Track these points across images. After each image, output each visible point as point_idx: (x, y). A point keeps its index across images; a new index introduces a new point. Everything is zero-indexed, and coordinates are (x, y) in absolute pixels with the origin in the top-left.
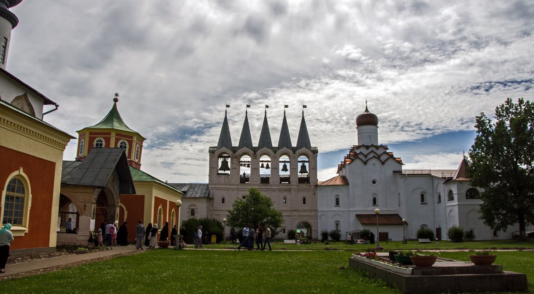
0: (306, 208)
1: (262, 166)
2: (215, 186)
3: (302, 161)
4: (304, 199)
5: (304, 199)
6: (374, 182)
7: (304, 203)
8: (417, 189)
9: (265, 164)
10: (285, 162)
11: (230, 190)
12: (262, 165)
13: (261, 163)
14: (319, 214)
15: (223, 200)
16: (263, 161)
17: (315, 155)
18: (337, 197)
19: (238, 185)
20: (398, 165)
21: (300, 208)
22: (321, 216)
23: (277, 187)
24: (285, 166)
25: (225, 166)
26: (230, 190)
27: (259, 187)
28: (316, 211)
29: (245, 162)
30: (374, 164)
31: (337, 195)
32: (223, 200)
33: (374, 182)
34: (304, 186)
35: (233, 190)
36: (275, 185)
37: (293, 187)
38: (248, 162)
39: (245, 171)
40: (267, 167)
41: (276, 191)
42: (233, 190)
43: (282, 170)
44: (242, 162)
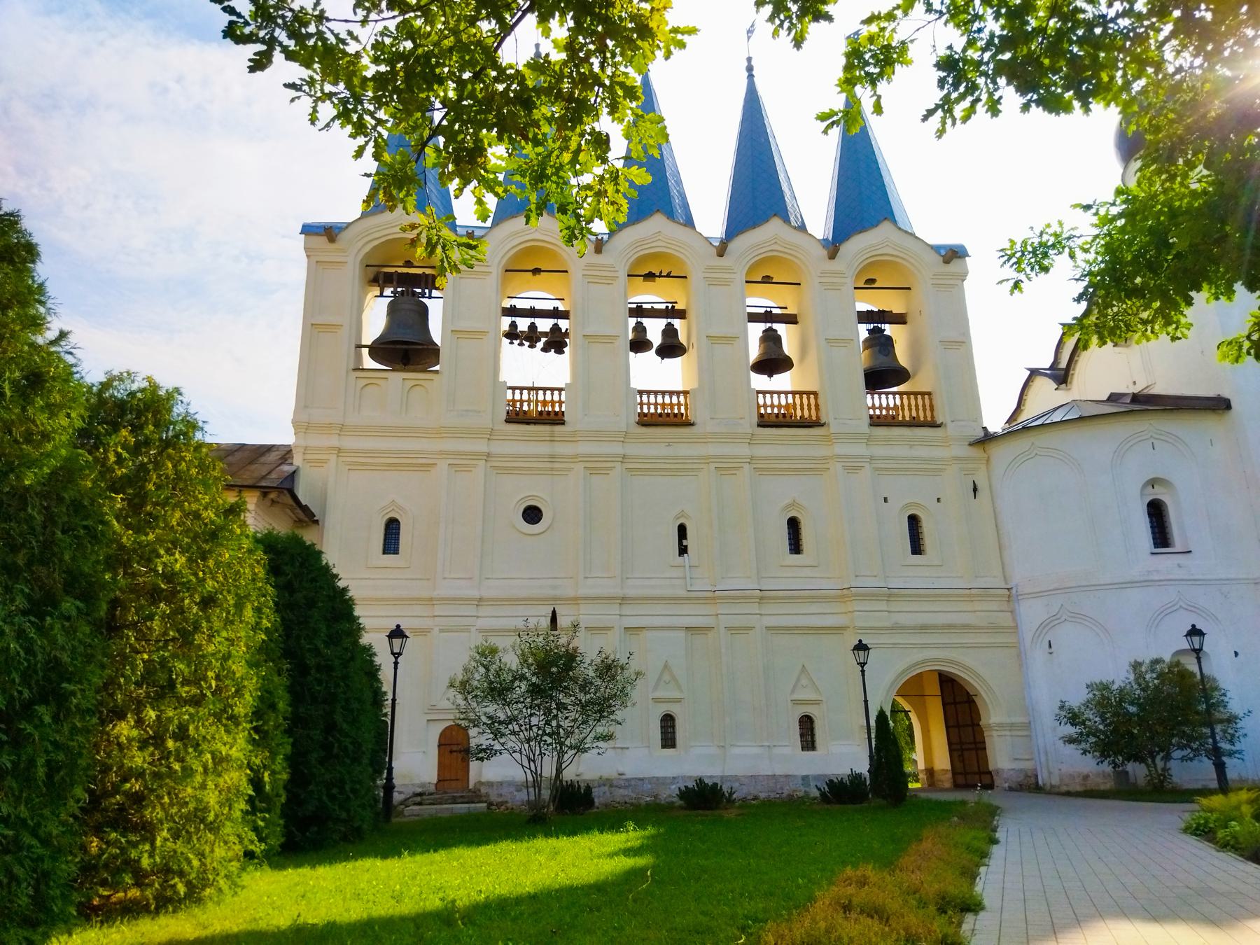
1: (640, 344)
2: (334, 441)
9: (655, 329)
10: (768, 317)
11: (443, 465)
12: (640, 329)
13: (632, 322)
14: (1032, 613)
15: (392, 529)
16: (638, 312)
17: (954, 266)
18: (1152, 494)
22: (1045, 626)
23: (744, 450)
24: (771, 339)
25: (406, 349)
26: (443, 465)
28: (1010, 596)
29: (533, 313)
31: (1153, 483)
32: (392, 529)
35: (460, 462)
37: (839, 449)
38: (555, 314)
39: (528, 369)
40: (671, 348)
42: (460, 462)
44: (512, 312)
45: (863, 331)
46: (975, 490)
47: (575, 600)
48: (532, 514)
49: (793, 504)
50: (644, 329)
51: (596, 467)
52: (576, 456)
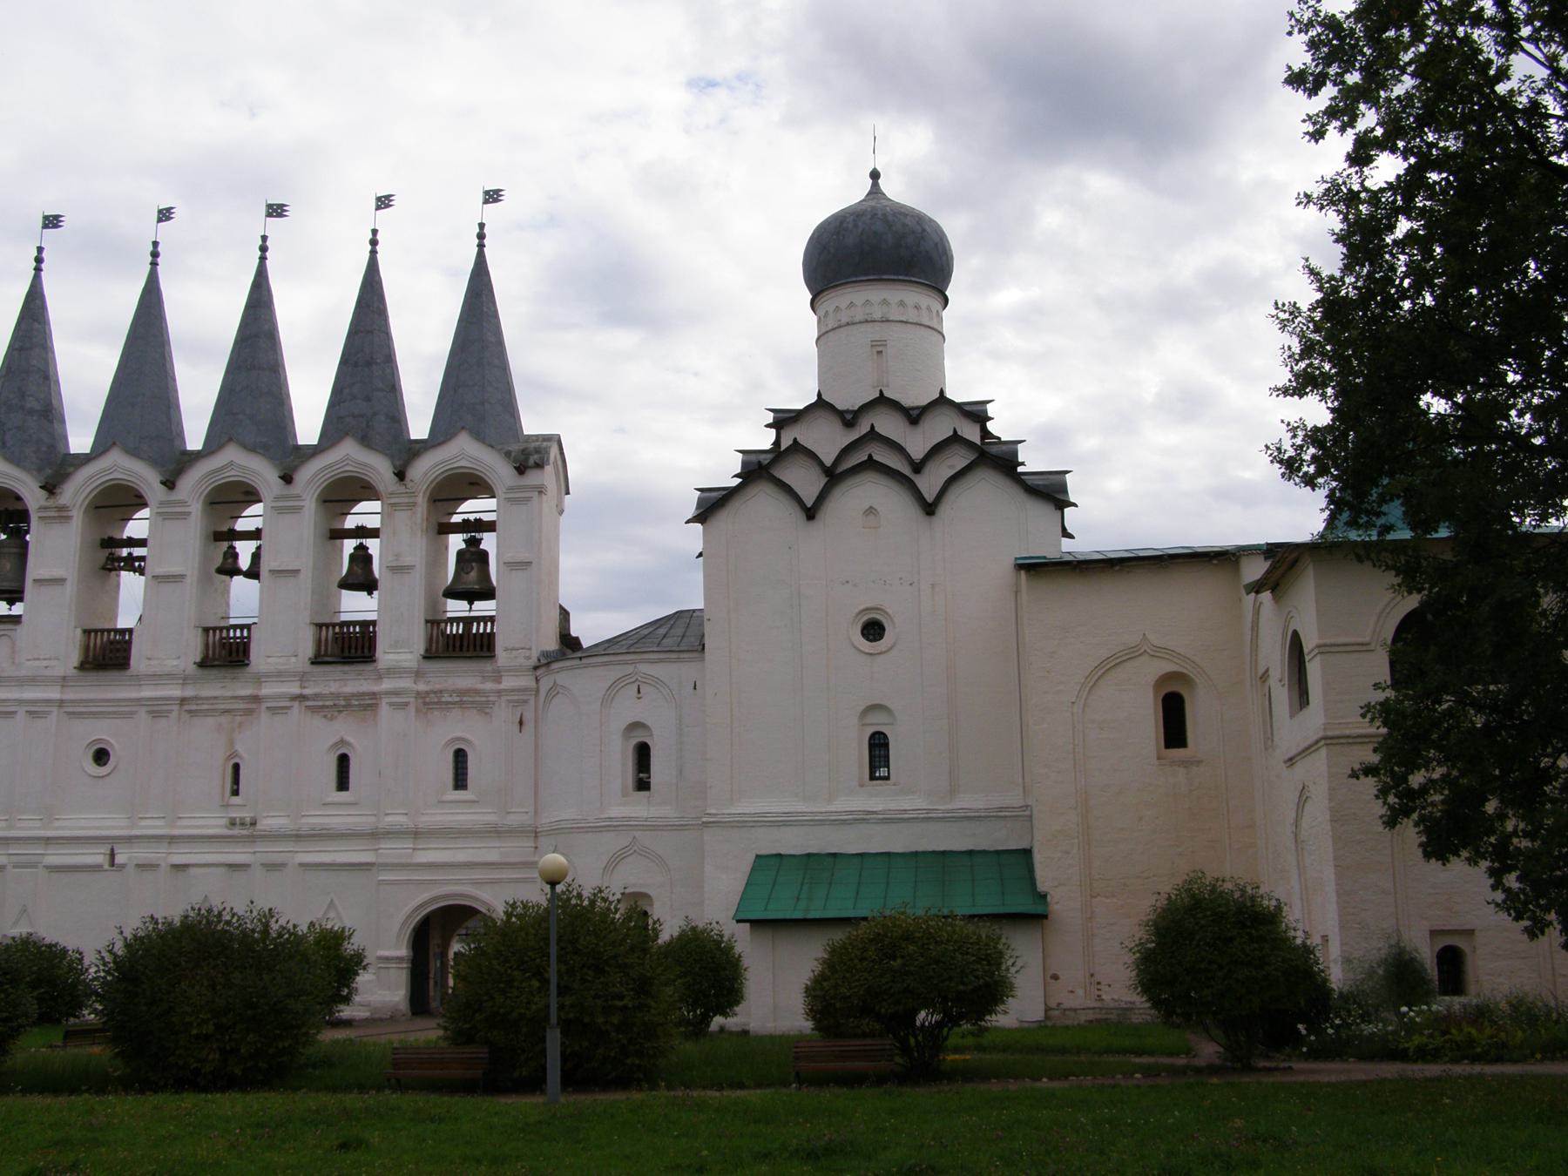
0: (654, 812)
3: (465, 526)
4: (460, 757)
5: (460, 757)
6: (874, 630)
7: (460, 782)
8: (1131, 654)
10: (362, 532)
11: (21, 715)
12: (233, 555)
17: (532, 478)
19: (64, 681)
20: (1039, 512)
21: (316, 819)
26: (21, 715)
27: (189, 692)
30: (871, 511)
31: (636, 726)
33: (874, 630)
34: (461, 676)
35: (36, 711)
36: (281, 676)
37: (386, 685)
41: (285, 709)
42: (36, 711)
43: (348, 584)
45: (456, 542)
46: (521, 723)
47: (129, 840)
48: (101, 756)
49: (342, 742)
50: (236, 556)
51: (157, 709)
52: (139, 700)
